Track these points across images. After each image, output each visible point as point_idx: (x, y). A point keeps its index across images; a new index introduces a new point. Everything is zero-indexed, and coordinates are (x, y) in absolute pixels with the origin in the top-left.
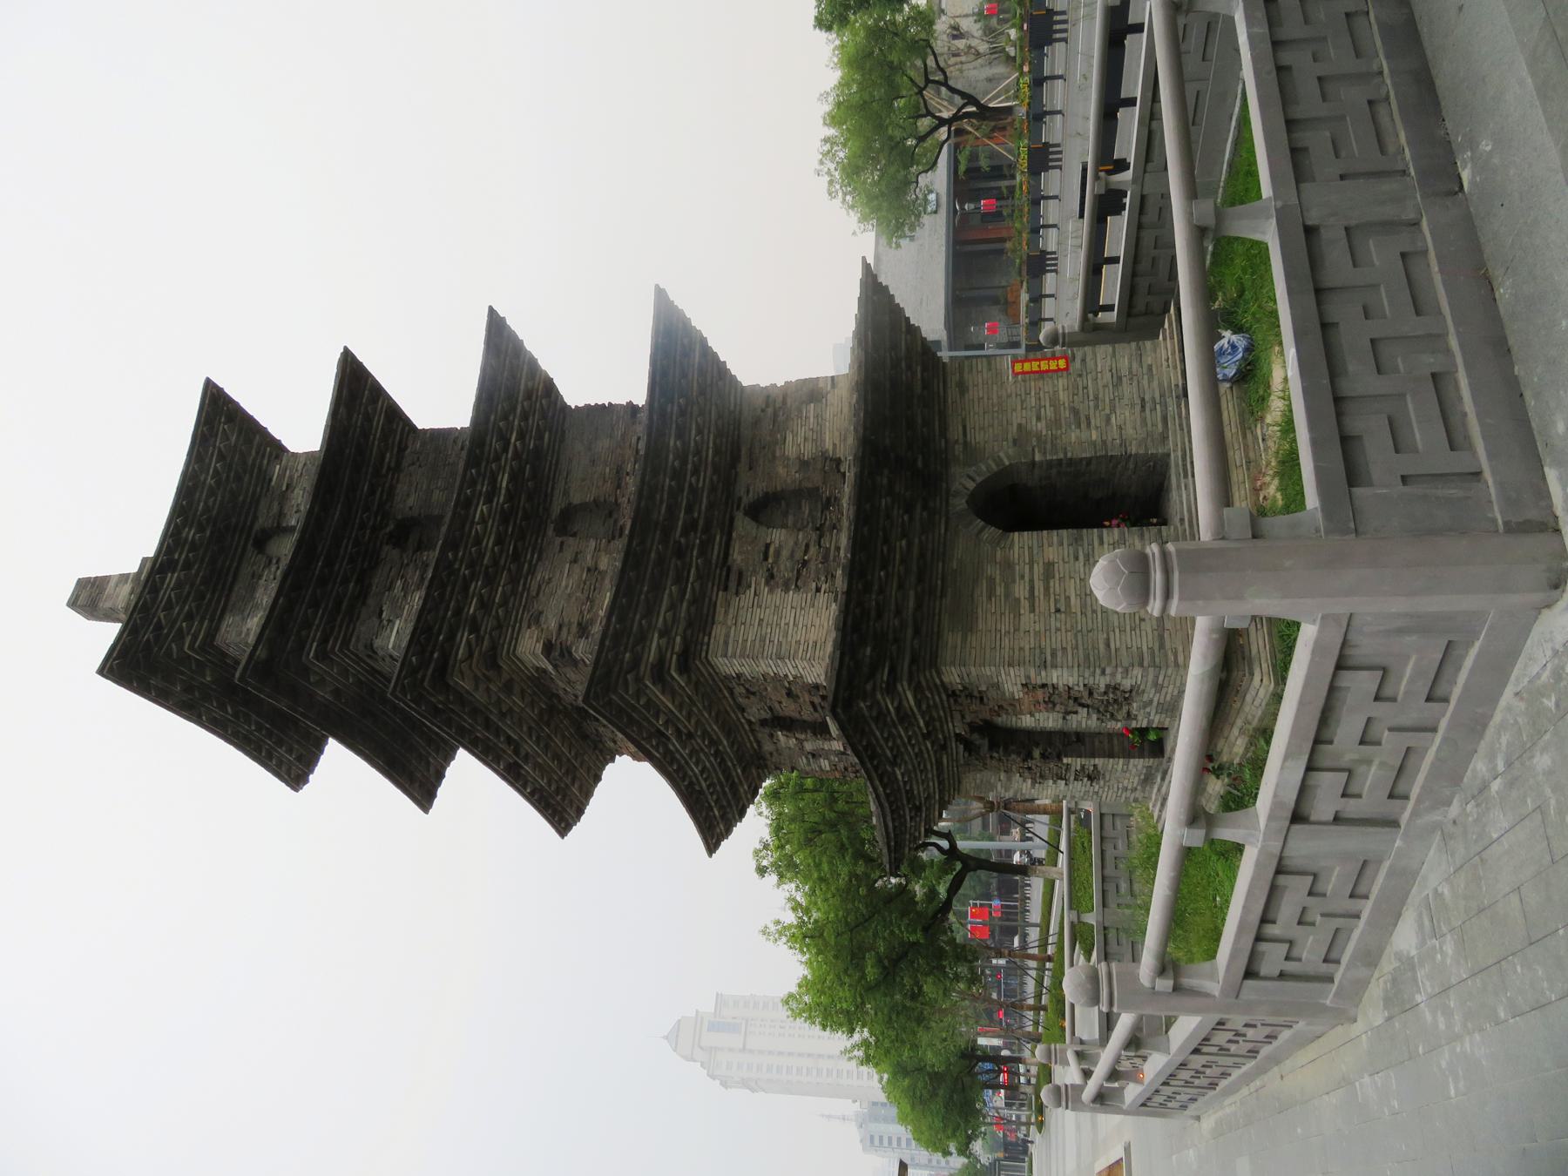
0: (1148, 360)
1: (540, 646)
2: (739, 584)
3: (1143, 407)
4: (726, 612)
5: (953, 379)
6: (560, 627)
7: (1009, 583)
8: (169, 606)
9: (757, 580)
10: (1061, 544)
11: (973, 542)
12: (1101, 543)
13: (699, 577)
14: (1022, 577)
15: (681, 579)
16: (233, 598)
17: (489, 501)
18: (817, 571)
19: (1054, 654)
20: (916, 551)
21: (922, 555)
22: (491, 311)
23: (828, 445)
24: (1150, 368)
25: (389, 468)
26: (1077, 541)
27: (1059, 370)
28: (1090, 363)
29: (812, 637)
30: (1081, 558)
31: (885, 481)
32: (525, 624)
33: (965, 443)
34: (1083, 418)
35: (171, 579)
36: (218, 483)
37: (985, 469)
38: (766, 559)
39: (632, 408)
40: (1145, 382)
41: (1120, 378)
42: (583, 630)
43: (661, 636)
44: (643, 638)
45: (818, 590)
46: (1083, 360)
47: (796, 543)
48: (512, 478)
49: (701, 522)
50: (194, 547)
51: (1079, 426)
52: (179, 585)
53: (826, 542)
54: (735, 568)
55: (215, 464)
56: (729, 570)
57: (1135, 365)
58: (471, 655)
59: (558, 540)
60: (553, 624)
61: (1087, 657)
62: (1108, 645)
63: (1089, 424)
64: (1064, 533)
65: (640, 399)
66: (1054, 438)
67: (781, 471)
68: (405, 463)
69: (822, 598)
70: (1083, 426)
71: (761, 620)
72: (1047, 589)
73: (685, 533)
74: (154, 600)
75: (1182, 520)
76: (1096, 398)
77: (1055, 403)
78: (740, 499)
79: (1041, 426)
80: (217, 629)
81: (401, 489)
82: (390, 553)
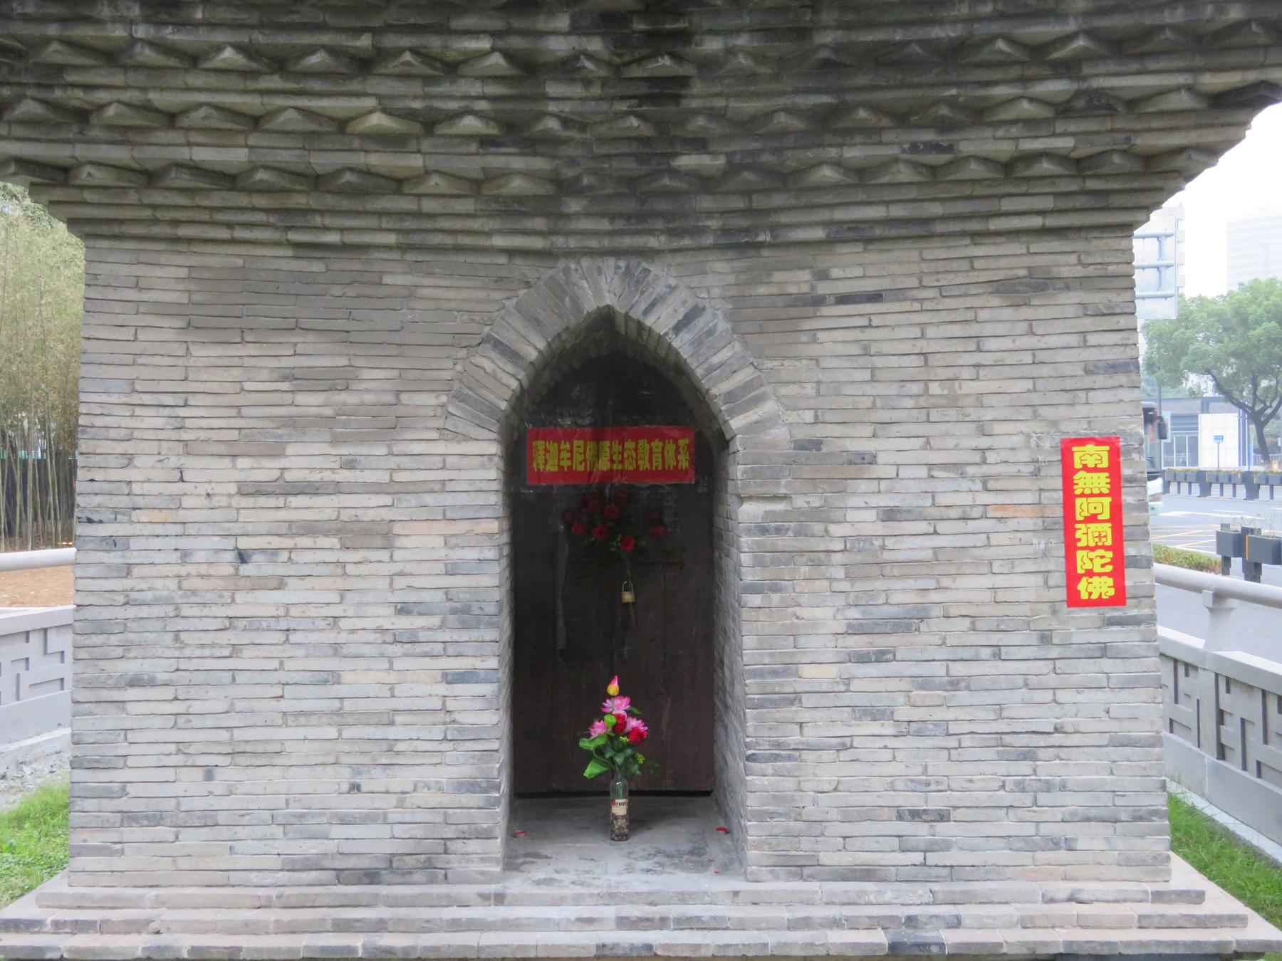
0: (1091, 839)
3: (916, 815)
5: (1062, 258)
7: (333, 427)
10: (452, 570)
12: (452, 678)
14: (350, 464)
19: (113, 543)
20: (378, 160)
21: (397, 184)
27: (1073, 578)
28: (1088, 670)
30: (404, 622)
31: (559, 46)
33: (819, 301)
34: (881, 642)
37: (717, 362)
40: (1009, 826)
41: (1028, 754)
46: (1104, 651)
51: (855, 630)
61: (101, 628)
62: (135, 682)
63: (862, 659)
66: (818, 560)
72: (310, 529)
75: (500, 899)
76: (954, 684)
77: (941, 563)
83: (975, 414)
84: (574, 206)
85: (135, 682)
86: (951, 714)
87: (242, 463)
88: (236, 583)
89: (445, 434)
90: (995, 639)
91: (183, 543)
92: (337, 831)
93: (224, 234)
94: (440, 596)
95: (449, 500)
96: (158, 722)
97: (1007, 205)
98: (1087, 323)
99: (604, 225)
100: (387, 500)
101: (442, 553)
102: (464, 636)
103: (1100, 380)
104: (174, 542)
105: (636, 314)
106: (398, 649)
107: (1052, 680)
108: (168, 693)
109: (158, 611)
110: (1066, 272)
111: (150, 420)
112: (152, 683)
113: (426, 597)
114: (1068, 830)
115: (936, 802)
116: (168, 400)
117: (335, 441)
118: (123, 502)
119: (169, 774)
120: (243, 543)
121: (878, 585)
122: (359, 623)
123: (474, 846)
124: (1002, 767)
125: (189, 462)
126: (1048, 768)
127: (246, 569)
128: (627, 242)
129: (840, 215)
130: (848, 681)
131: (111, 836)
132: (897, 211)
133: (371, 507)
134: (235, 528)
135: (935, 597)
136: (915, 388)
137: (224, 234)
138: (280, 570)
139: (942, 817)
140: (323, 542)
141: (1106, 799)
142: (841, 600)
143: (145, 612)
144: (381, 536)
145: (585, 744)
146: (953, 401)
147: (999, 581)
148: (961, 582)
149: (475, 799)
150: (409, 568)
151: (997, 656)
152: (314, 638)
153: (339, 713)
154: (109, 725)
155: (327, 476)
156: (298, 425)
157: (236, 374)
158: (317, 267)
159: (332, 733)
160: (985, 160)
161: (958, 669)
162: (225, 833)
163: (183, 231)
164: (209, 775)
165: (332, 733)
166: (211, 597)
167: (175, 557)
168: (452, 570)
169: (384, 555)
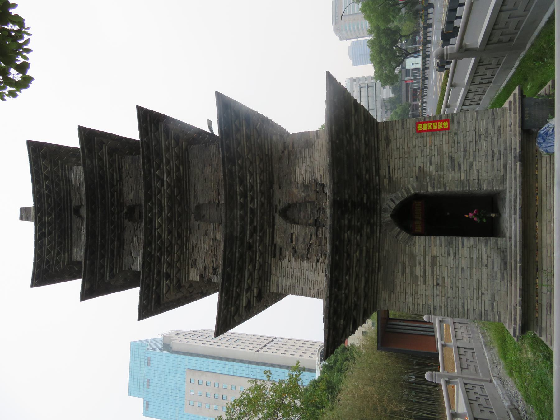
0: (498, 123)
2: (281, 254)
3: (493, 157)
4: (276, 269)
5: (382, 134)
6: (205, 268)
8: (49, 252)
9: (289, 253)
10: (441, 245)
11: (393, 237)
12: (463, 246)
13: (261, 254)
14: (420, 264)
15: (252, 260)
16: (74, 240)
17: (160, 215)
19: (435, 309)
20: (364, 255)
21: (368, 252)
23: (317, 176)
25: (117, 181)
26: (450, 243)
27: (444, 129)
28: (462, 125)
29: (317, 287)
31: (346, 222)
32: (190, 266)
33: (390, 177)
34: (456, 164)
36: (50, 191)
37: (401, 195)
38: (292, 241)
40: (495, 139)
41: (480, 136)
42: (215, 270)
43: (247, 293)
44: (239, 296)
45: (318, 261)
46: (459, 123)
47: (305, 234)
48: (170, 198)
49: (258, 227)
50: (50, 224)
51: (454, 170)
52: (49, 242)
53: (319, 232)
54: (278, 246)
55: (45, 183)
56: (275, 245)
58: (169, 288)
59: (197, 223)
60: (201, 266)
61: (452, 312)
62: (463, 307)
63: (460, 168)
64: (443, 238)
66: (440, 177)
67: (295, 191)
68: (124, 175)
69: (320, 266)
70: (457, 169)
71: (292, 275)
72: (432, 271)
73: (251, 236)
74: (42, 252)
75: (510, 238)
76: (465, 150)
77: (441, 153)
78: (276, 206)
79: (432, 169)
80: (72, 254)
81: (125, 190)
82: (128, 224)
83: (411, 149)
84: (372, 221)
86: (471, 151)
87: (419, 283)
89: (414, 245)
90: (456, 143)
92: (496, 269)
93: (376, 284)
94: (446, 248)
95: (427, 246)
96: (472, 303)
97: (373, 144)
99: (375, 216)
101: (438, 247)
102: (454, 243)
103: (405, 126)
104: (435, 297)
105: (392, 210)
106: (457, 256)
107: (464, 132)
108: (466, 301)
109: (449, 301)
110: (385, 133)
111: (411, 300)
112: (464, 303)
113: (446, 251)
114: (496, 128)
115: (490, 153)
116: (407, 296)
117: (415, 266)
118: (427, 306)
119: (483, 301)
120: (435, 284)
121: (445, 165)
122: (452, 263)
123: (499, 243)
124: (483, 141)
125: (419, 293)
126: (483, 132)
127: (441, 284)
128: (378, 212)
130: (464, 171)
132: (374, 164)
133: (428, 260)
134: (432, 285)
135: (447, 155)
136: (406, 160)
137: (376, 284)
139: (493, 152)
140: (435, 269)
141: (490, 120)
142: (448, 172)
143: (449, 304)
144: (434, 258)
145: (479, 222)
146: (409, 153)
147: (444, 143)
148: (444, 150)
149: (489, 243)
150: (441, 253)
151: (459, 143)
152: (454, 272)
153: (470, 268)
155: (422, 268)
156: (412, 272)
157: (402, 284)
158: (382, 268)
159: (474, 270)
160: (365, 149)
161: (462, 150)
162: (496, 291)
163: (375, 291)
164: (483, 294)
165: (474, 270)
166: (446, 291)
167: (438, 297)
168: (441, 245)
169: (438, 258)
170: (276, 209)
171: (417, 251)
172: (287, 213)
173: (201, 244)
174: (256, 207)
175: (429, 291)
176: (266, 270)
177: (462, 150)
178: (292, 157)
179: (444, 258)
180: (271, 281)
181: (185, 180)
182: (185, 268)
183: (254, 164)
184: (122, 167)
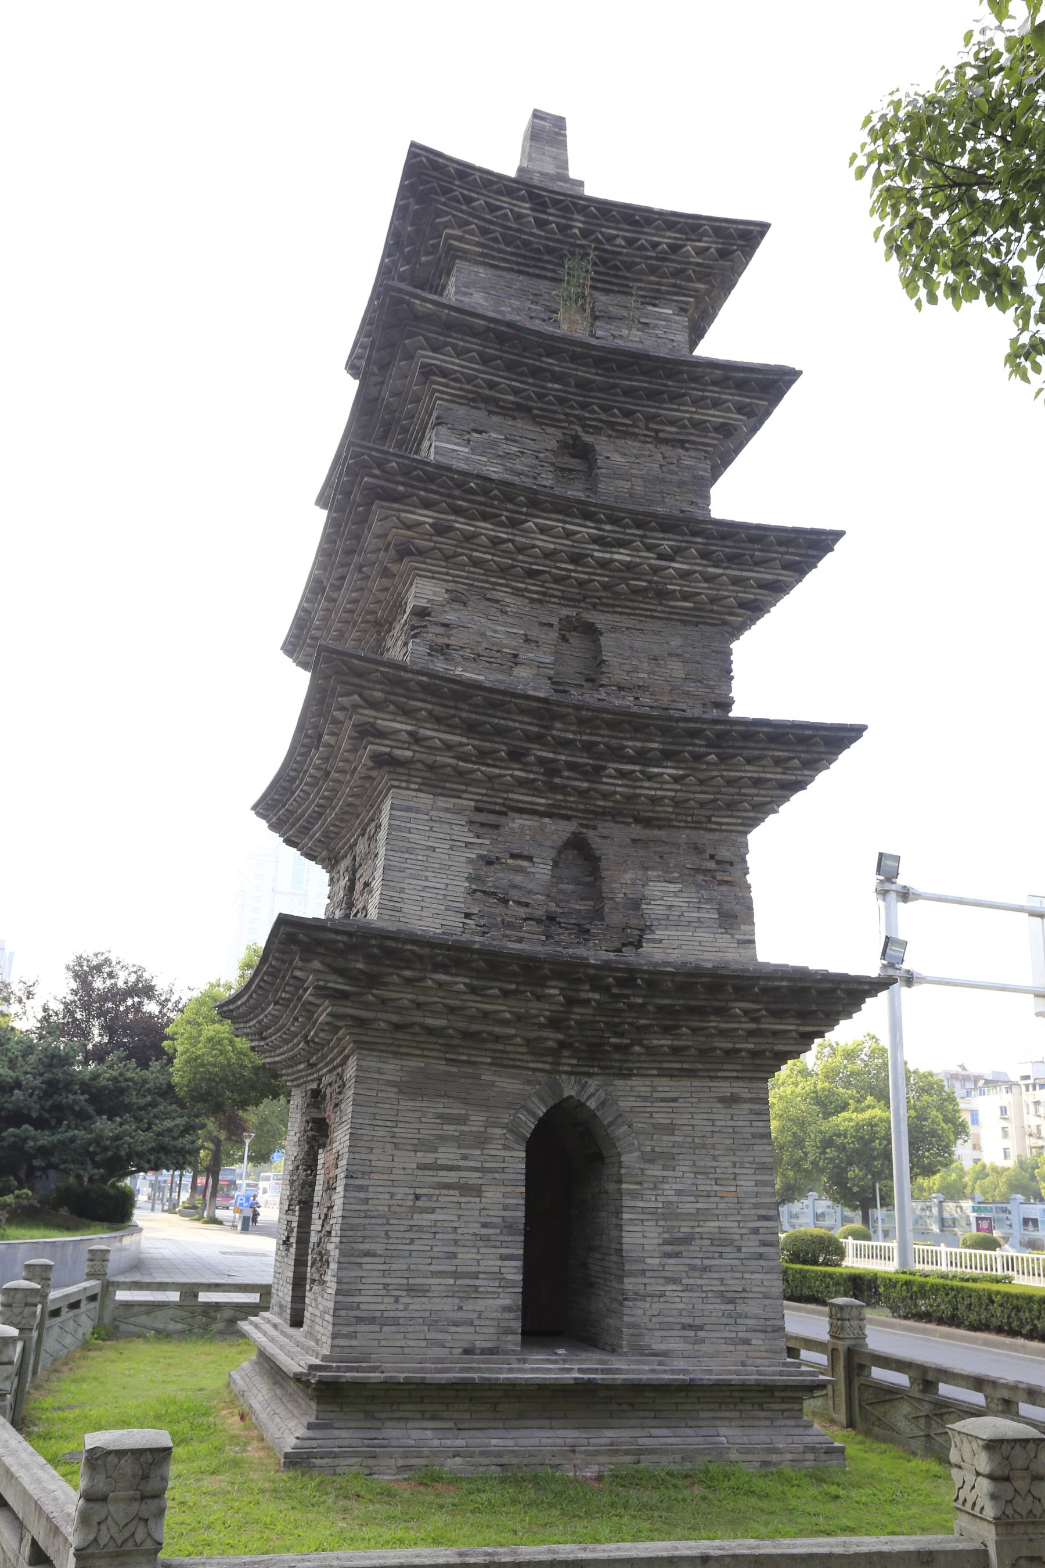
1: (423, 603)
2: (482, 825)
4: (447, 810)
5: (742, 1089)
7: (459, 1141)
8: (492, 208)
9: (485, 846)
10: (506, 1208)
11: (519, 1097)
12: (504, 1257)
13: (490, 778)
14: (465, 1158)
15: (483, 757)
16: (508, 276)
17: (595, 540)
18: (491, 916)
19: (362, 1188)
20: (497, 1030)
21: (497, 1038)
22: (838, 535)
23: (659, 934)
24: (747, 1342)
25: (657, 431)
26: (508, 1228)
29: (407, 908)
30: (484, 1231)
32: (451, 586)
34: (676, 1248)
35: (525, 208)
36: (643, 248)
38: (513, 856)
39: (727, 704)
41: (732, 1301)
42: (441, 650)
43: (409, 733)
44: (407, 713)
45: (467, 916)
46: (761, 1256)
48: (629, 567)
50: (564, 229)
51: (666, 1243)
52: (519, 217)
53: (530, 926)
54: (502, 820)
55: (665, 240)
56: (505, 814)
57: (749, 1321)
58: (409, 527)
59: (555, 621)
60: (451, 617)
61: (353, 1228)
62: (368, 1254)
63: (669, 1256)
64: (521, 1213)
65: (736, 712)
67: (628, 876)
68: (664, 448)
69: (455, 921)
70: (668, 1248)
71: (434, 849)
76: (705, 1269)
78: (595, 828)
81: (633, 446)
82: (550, 439)
83: (712, 1152)
84: (566, 1053)
85: (368, 1254)
86: (703, 1282)
87: (419, 1154)
88: (414, 1210)
89: (506, 1147)
90: (720, 1249)
91: (392, 1190)
92: (453, 1329)
93: (419, 1052)
94: (500, 1220)
95: (505, 1176)
96: (376, 1274)
97: (725, 1067)
98: (752, 1117)
99: (574, 1062)
100: (479, 1175)
101: (502, 1200)
102: (510, 1238)
103: (758, 1141)
104: (387, 1189)
105: (583, 1100)
106: (481, 1243)
107: (742, 1268)
108: (382, 1260)
109: (379, 1221)
110: (745, 1096)
112: (374, 1255)
113: (494, 1220)
114: (748, 1335)
115: (698, 1322)
116: (389, 1124)
117: (459, 1147)
118: (368, 1169)
119: (379, 1299)
120: (418, 1191)
121: (676, 1223)
122: (466, 1231)
123: (510, 1338)
124: (723, 1307)
125: (396, 1152)
126: (741, 1308)
127: (419, 1203)
128: (582, 1069)
129: (665, 1065)
131: (352, 1329)
132: (686, 1066)
133: (473, 1178)
134: (415, 1184)
135: (698, 1230)
136: (689, 1139)
137: (419, 1052)
138: (433, 1205)
139: (700, 1328)
140: (452, 1192)
141: (762, 1322)
142: (661, 1230)
143: (373, 1221)
144: (476, 1191)
146: (703, 1146)
147: (722, 1224)
148: (708, 1224)
149: (512, 1315)
150: (488, 1206)
151: (721, 1257)
152: (446, 1237)
153: (455, 1272)
154: (354, 1274)
155: (455, 1163)
156: (443, 1138)
157: (418, 1114)
158: (455, 1070)
159: (452, 1282)
160: (721, 1049)
161: (706, 1262)
162: (402, 1329)
163: (402, 1050)
164: (397, 1299)
165: (452, 1282)
166: (403, 1215)
167: (388, 1196)
168: (506, 1208)
169: (477, 1200)
170: (587, 826)
171: (493, 1152)
172: (580, 852)
173: (505, 624)
174: (605, 780)
175: (403, 1177)
176: (448, 785)
177: (706, 1262)
178: (700, 878)
179: (477, 1213)
180: (420, 794)
181: (659, 608)
182: (447, 574)
183: (699, 789)
184: (687, 450)
